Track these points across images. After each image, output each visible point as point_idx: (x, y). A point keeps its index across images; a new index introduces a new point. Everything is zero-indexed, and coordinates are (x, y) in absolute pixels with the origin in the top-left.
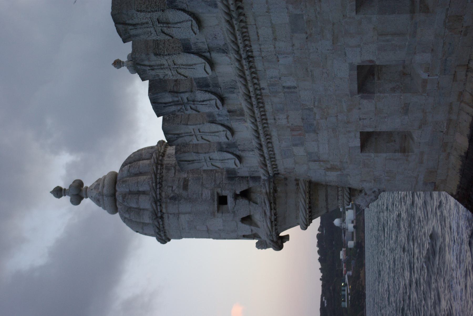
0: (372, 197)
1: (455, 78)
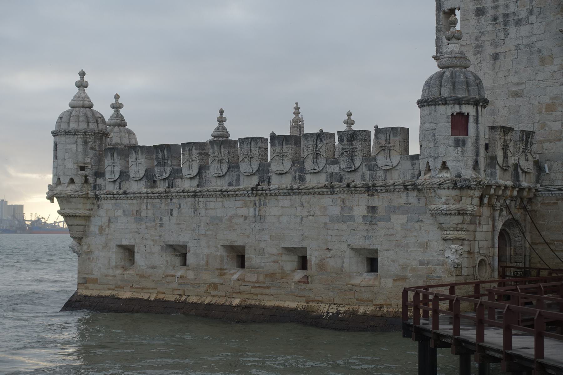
1: (174, 289)
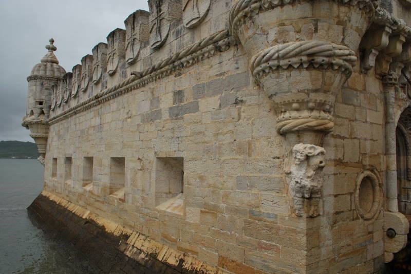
0: (42, 162)
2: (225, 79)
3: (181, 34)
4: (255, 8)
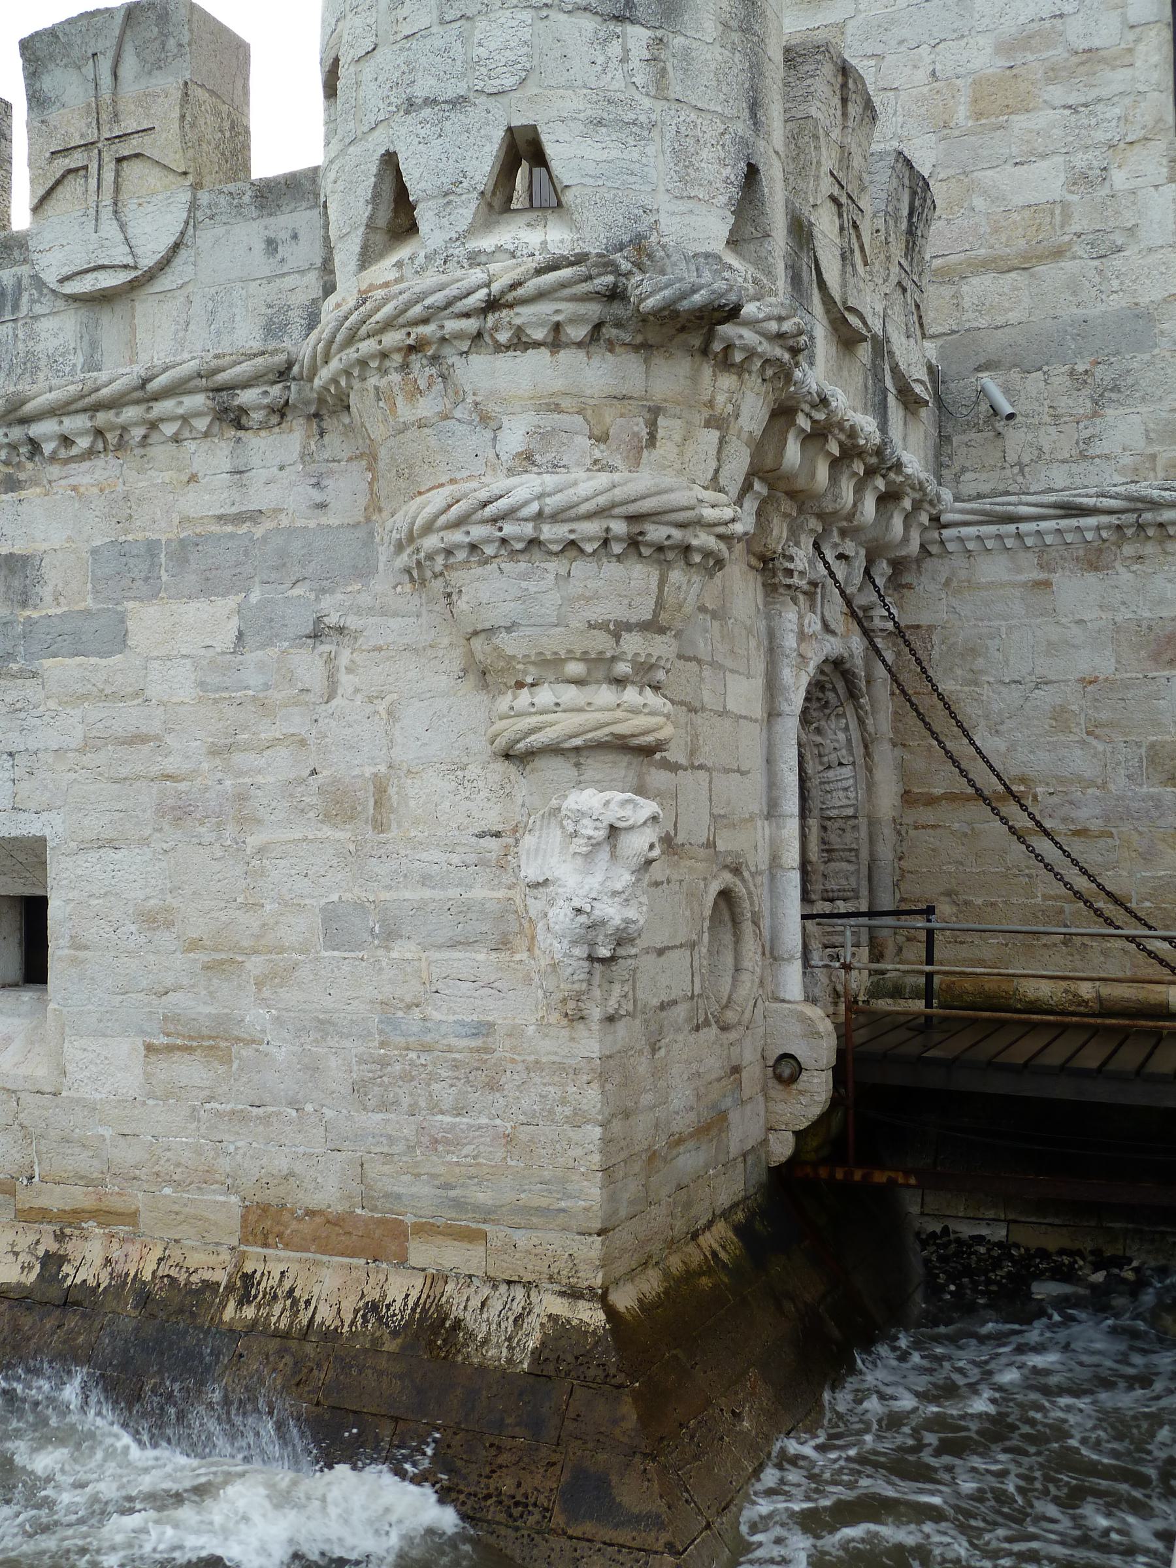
2: (264, 539)
3: (16, 307)
4: (459, 336)
